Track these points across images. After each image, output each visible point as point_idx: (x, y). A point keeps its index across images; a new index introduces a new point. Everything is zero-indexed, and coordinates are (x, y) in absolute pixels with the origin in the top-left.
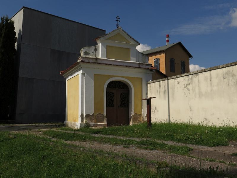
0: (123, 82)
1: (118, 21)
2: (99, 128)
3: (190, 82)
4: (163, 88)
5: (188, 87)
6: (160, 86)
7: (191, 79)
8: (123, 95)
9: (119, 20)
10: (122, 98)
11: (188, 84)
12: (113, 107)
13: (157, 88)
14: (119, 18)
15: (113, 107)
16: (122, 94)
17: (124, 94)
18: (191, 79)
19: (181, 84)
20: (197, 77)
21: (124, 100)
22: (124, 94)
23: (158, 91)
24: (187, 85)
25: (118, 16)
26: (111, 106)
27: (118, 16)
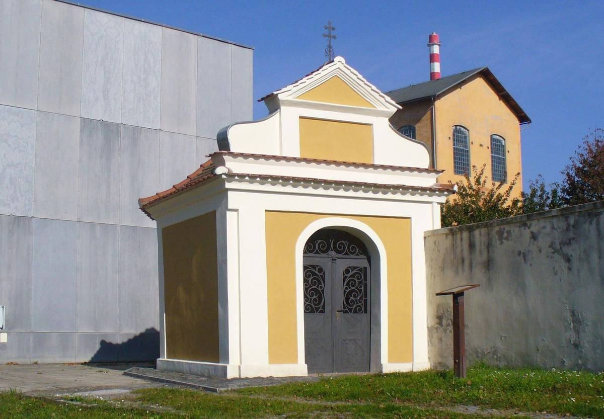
0: (460, 314)
1: (329, 36)
2: (353, 374)
3: (571, 235)
4: (481, 252)
5: (568, 250)
6: (472, 246)
7: (573, 226)
8: (351, 273)
9: (333, 33)
10: (348, 284)
11: (568, 243)
12: (323, 312)
13: (462, 250)
14: (333, 29)
15: (323, 312)
16: (347, 271)
17: (354, 271)
18: (573, 226)
19: (544, 242)
20: (594, 222)
21: (353, 291)
22: (354, 271)
23: (467, 263)
24: (563, 243)
25: (329, 23)
26: (317, 309)
27: (329, 23)
